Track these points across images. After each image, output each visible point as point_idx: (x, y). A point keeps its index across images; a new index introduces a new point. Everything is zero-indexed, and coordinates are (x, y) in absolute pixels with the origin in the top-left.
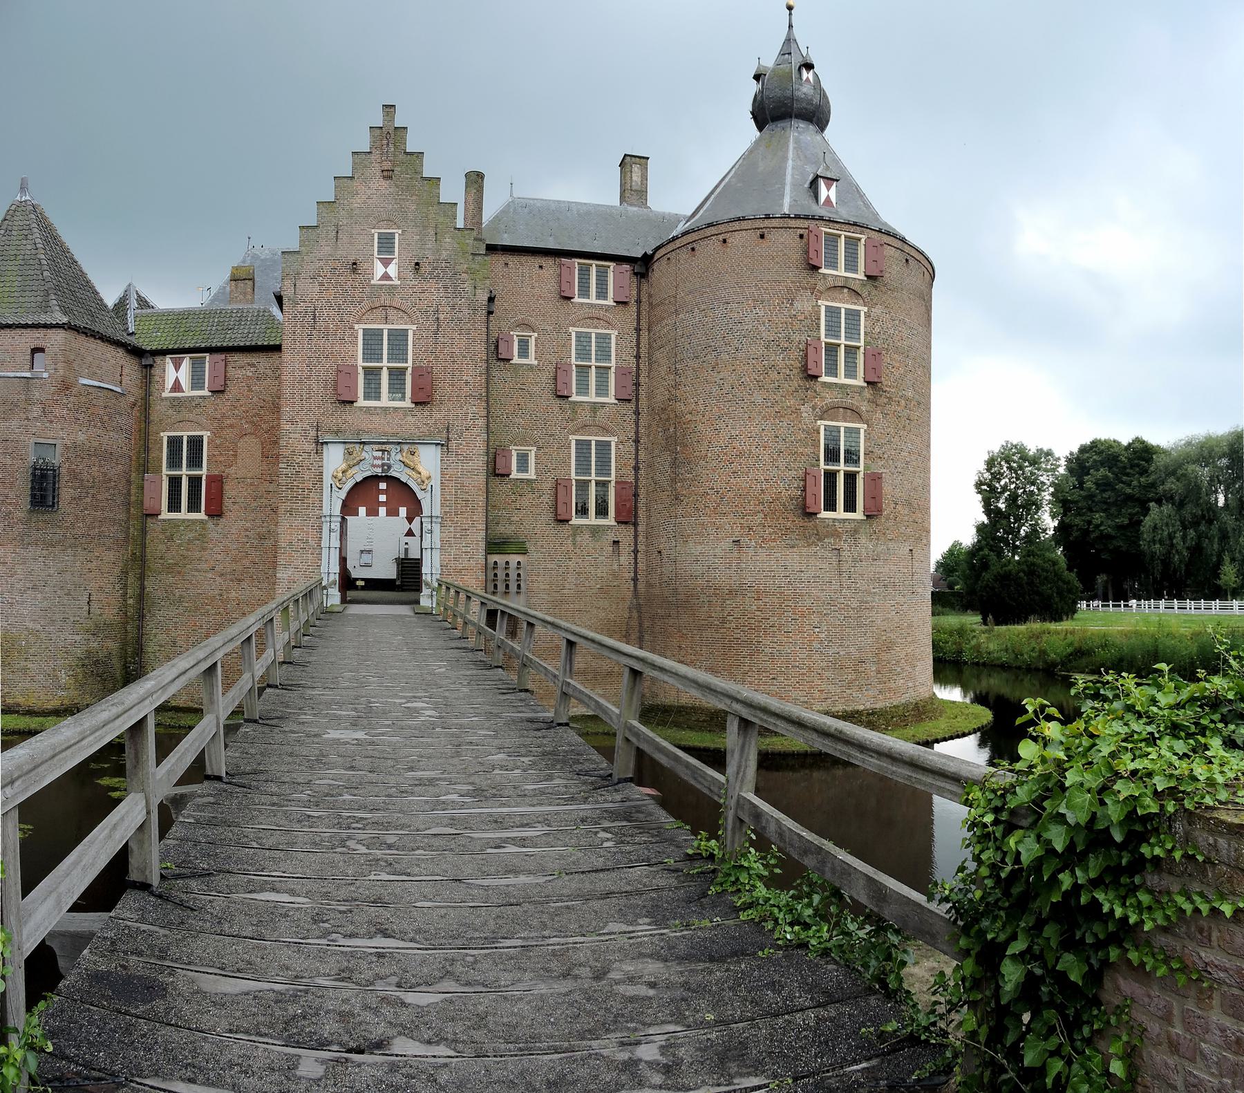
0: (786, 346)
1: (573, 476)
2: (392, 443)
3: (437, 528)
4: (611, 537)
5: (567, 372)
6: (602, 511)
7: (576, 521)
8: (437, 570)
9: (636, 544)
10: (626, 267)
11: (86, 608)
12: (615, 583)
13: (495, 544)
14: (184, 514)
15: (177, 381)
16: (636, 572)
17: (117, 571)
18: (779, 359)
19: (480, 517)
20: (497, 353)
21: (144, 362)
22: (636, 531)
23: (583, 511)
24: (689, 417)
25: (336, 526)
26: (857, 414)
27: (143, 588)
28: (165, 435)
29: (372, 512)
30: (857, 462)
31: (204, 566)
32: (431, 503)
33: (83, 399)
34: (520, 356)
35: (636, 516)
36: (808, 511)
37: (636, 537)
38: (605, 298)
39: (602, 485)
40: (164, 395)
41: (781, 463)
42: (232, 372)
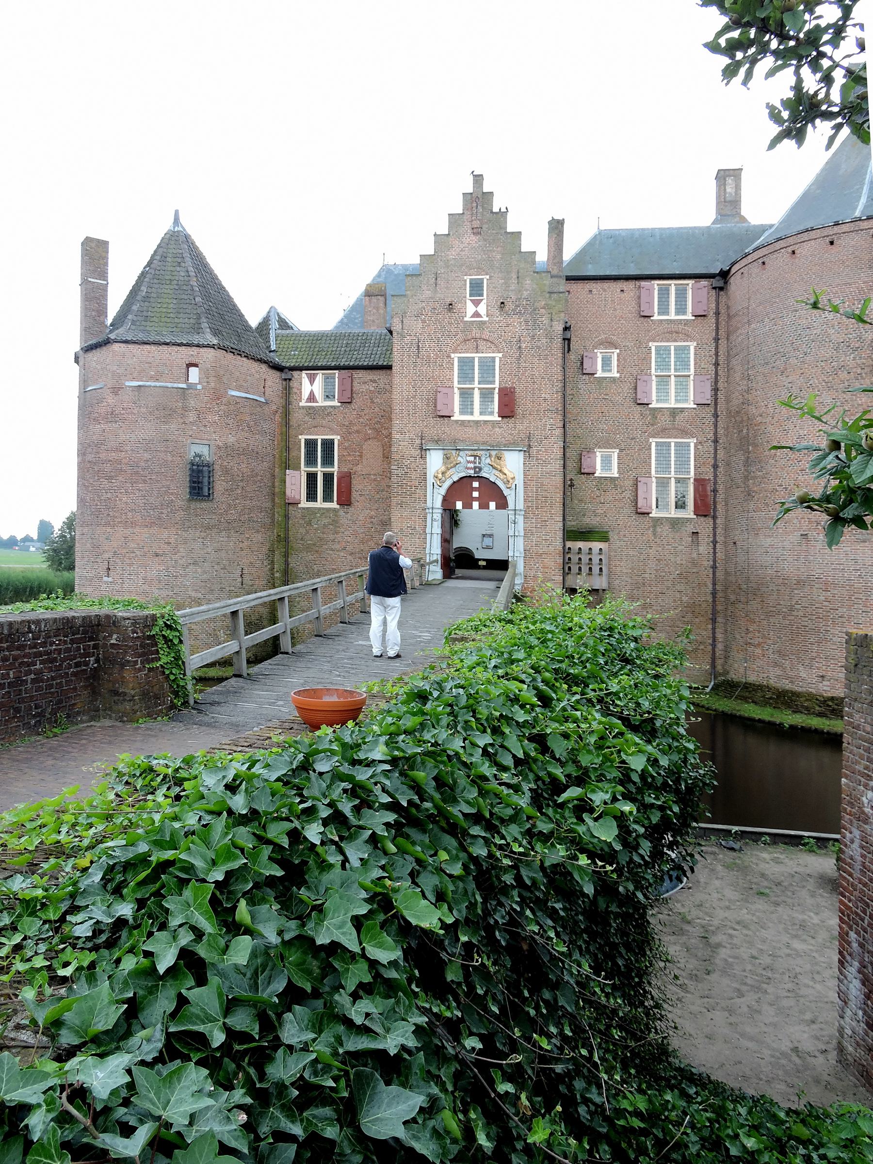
0: (857, 345)
2: (483, 450)
10: (704, 283)
11: (240, 580)
12: (694, 570)
13: (582, 532)
17: (265, 550)
18: (849, 360)
24: (759, 419)
27: (287, 563)
31: (337, 546)
33: (232, 408)
34: (603, 370)
38: (684, 313)
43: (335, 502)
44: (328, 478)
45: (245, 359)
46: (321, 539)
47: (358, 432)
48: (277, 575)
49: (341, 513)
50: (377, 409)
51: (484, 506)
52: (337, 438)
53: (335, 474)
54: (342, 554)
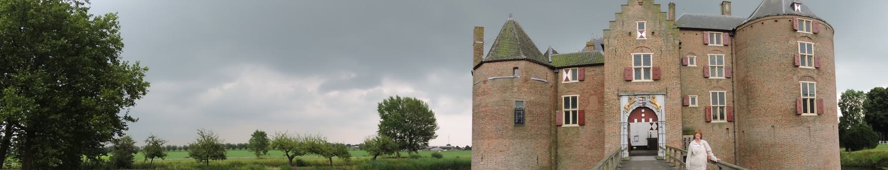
1: (711, 105)
3: (664, 126)
4: (726, 127)
5: (708, 68)
6: (722, 117)
7: (713, 122)
8: (664, 142)
9: (734, 129)
14: (571, 125)
15: (567, 77)
16: (735, 140)
17: (547, 147)
19: (680, 120)
20: (682, 63)
21: (555, 71)
22: (734, 124)
23: (715, 118)
25: (626, 126)
26: (812, 78)
28: (563, 97)
29: (639, 121)
30: (814, 95)
32: (661, 117)
34: (690, 64)
35: (734, 119)
36: (798, 113)
37: (734, 126)
39: (722, 108)
40: (562, 82)
41: (787, 97)
42: (586, 73)
43: (578, 124)
44: (574, 113)
45: (535, 64)
46: (572, 141)
47: (587, 92)
48: (553, 158)
49: (580, 128)
50: (595, 82)
51: (647, 120)
52: (578, 96)
53: (578, 111)
54: (581, 147)
